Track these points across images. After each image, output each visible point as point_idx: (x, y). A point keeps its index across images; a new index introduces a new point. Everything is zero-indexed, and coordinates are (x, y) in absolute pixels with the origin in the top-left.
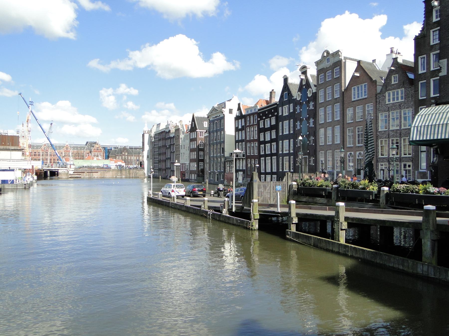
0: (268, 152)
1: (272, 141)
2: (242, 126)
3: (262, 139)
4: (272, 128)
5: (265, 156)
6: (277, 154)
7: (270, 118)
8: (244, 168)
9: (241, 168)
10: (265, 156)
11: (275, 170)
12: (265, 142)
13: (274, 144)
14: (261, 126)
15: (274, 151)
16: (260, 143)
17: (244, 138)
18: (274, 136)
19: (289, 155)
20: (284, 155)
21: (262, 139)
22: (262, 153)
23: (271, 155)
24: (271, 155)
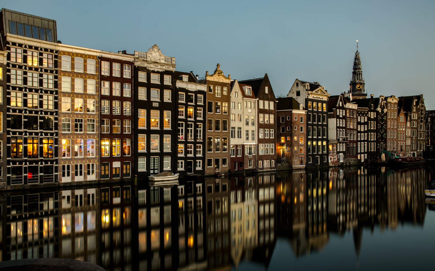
0: (362, 139)
1: (364, 132)
2: (343, 116)
3: (359, 130)
4: (365, 123)
5: (361, 141)
6: (367, 141)
7: (364, 116)
8: (344, 150)
9: (341, 150)
10: (361, 141)
11: (366, 150)
12: (360, 132)
13: (366, 134)
14: (359, 120)
15: (366, 139)
16: (358, 132)
17: (344, 126)
18: (366, 129)
19: (374, 141)
20: (371, 141)
21: (359, 130)
22: (359, 139)
23: (364, 141)
24: (364, 141)
